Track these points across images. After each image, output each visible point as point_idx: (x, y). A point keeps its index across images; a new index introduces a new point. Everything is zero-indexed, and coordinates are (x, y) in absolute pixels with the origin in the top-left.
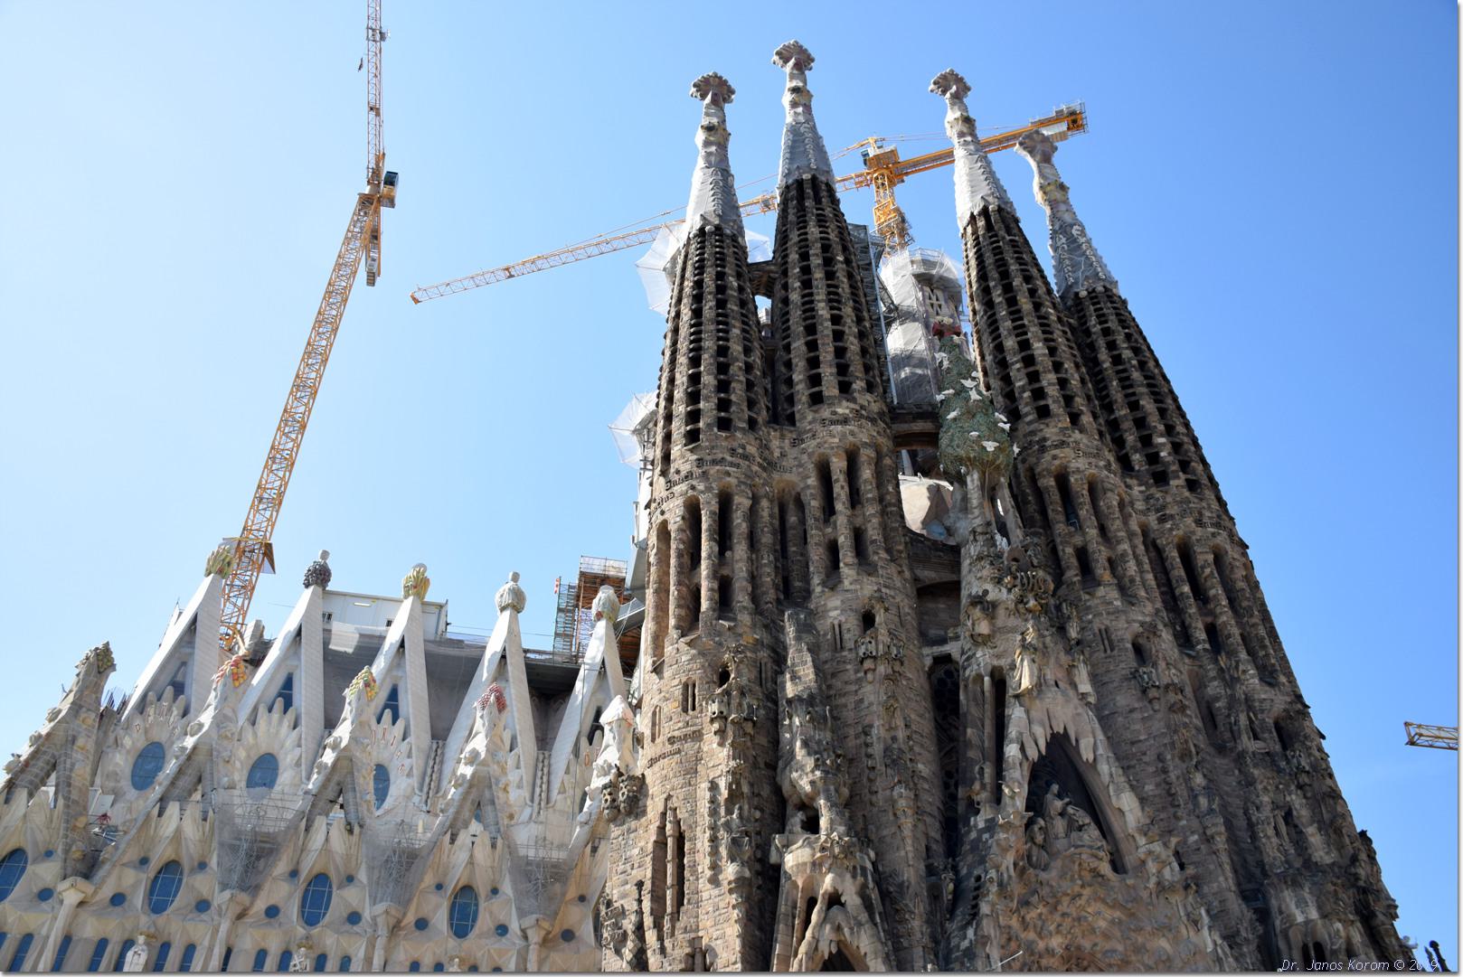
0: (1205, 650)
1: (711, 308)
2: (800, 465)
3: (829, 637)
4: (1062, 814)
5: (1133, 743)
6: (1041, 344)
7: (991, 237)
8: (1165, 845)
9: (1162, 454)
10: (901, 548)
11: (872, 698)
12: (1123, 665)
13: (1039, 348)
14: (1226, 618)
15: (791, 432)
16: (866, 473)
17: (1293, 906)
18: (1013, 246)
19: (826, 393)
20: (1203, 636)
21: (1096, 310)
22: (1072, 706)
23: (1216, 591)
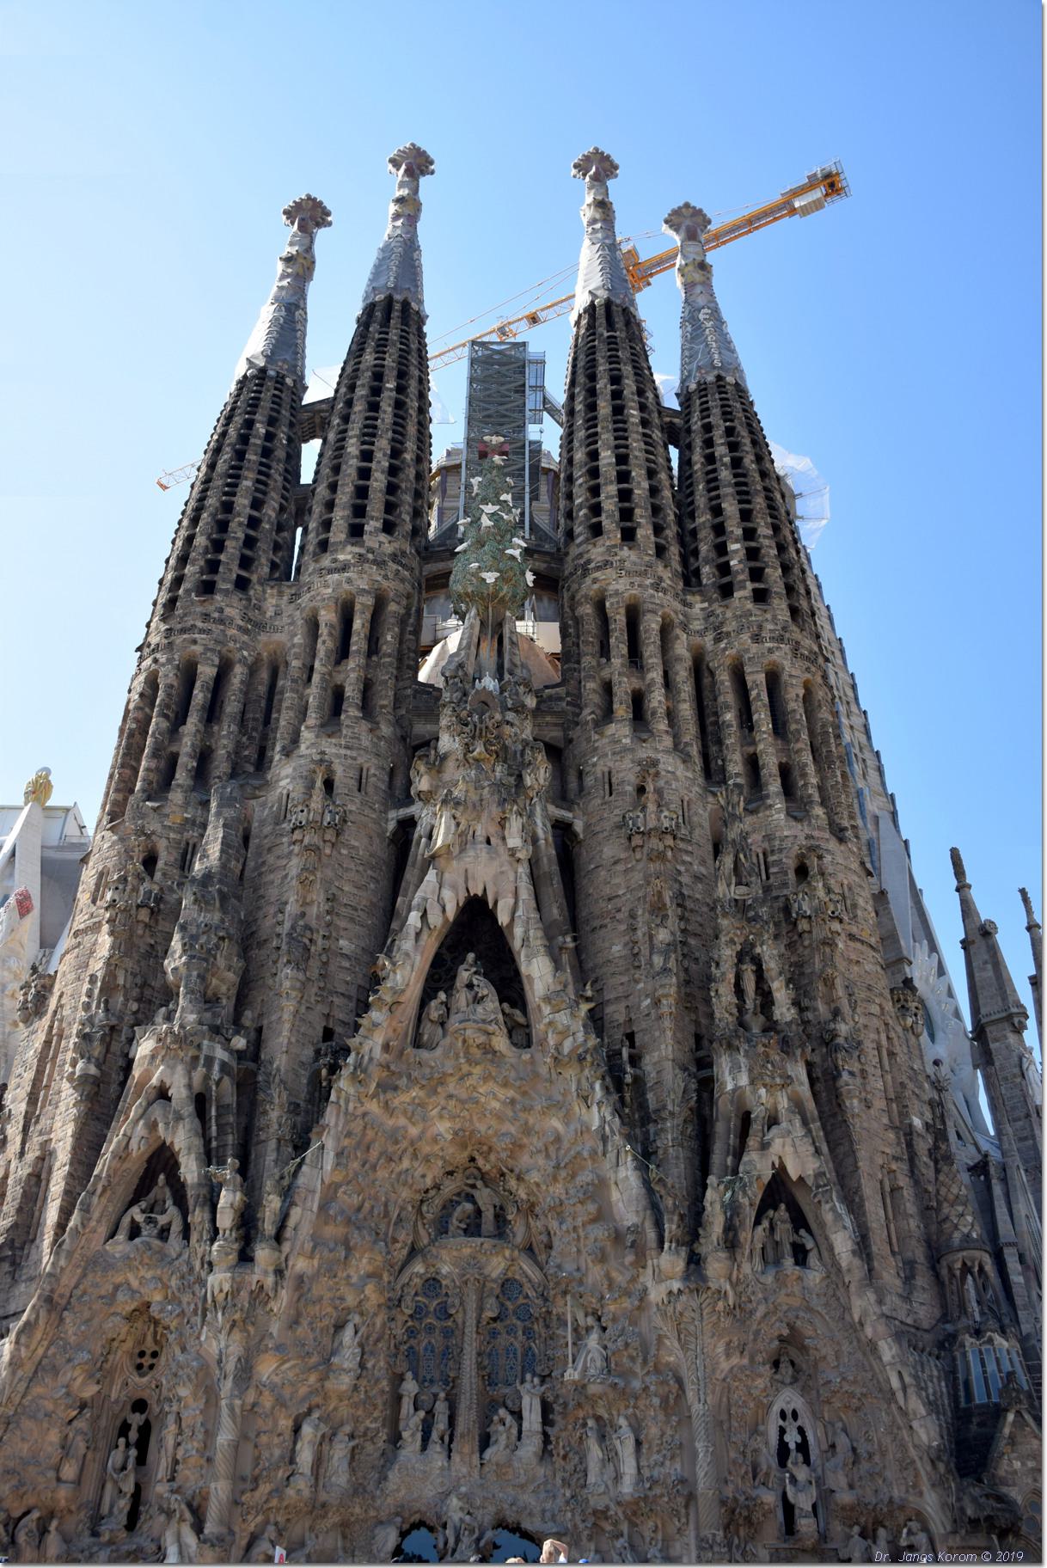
4: (470, 986)
5: (610, 899)
6: (609, 452)
8: (573, 1015)
9: (732, 563)
10: (385, 702)
12: (617, 812)
13: (607, 457)
17: (727, 1073)
19: (332, 540)
22: (496, 863)
23: (762, 717)
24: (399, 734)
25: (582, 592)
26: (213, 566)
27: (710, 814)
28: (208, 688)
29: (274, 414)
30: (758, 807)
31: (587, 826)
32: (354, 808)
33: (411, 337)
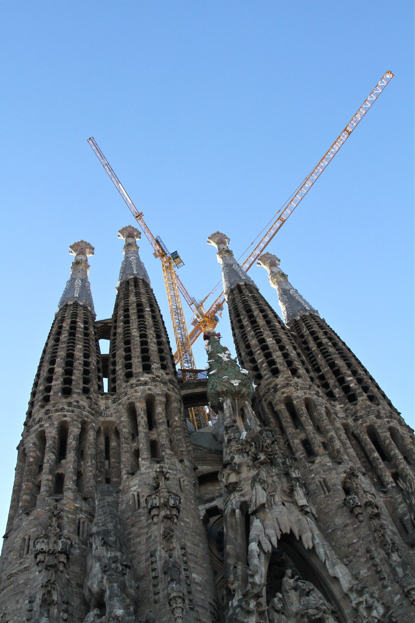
0: (392, 487)
1: (65, 337)
2: (117, 412)
3: (131, 503)
4: (295, 588)
5: (349, 546)
6: (271, 339)
7: (240, 297)
9: (351, 385)
11: (156, 533)
12: (337, 499)
14: (403, 465)
16: (159, 409)
18: (253, 298)
20: (391, 479)
21: (305, 325)
31: (319, 511)
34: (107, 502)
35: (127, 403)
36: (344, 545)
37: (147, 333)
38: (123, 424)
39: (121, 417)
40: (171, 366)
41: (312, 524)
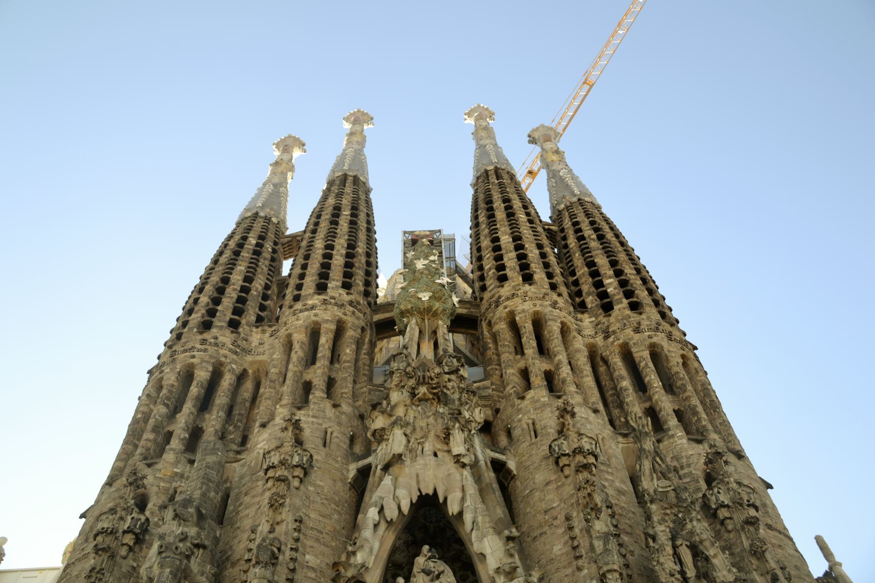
1: (226, 257)
3: (252, 464)
4: (427, 572)
5: (546, 512)
6: (507, 236)
9: (609, 290)
13: (506, 240)
15: (270, 326)
16: (325, 341)
23: (652, 378)
24: (357, 413)
25: (498, 314)
26: (212, 313)
27: (622, 451)
28: (201, 386)
29: (263, 234)
30: (663, 437)
31: (519, 465)
32: (319, 458)
33: (360, 193)
34: (208, 463)
35: (284, 335)
36: (540, 511)
37: (334, 243)
38: (273, 362)
39: (274, 353)
40: (361, 284)
41: (468, 481)
